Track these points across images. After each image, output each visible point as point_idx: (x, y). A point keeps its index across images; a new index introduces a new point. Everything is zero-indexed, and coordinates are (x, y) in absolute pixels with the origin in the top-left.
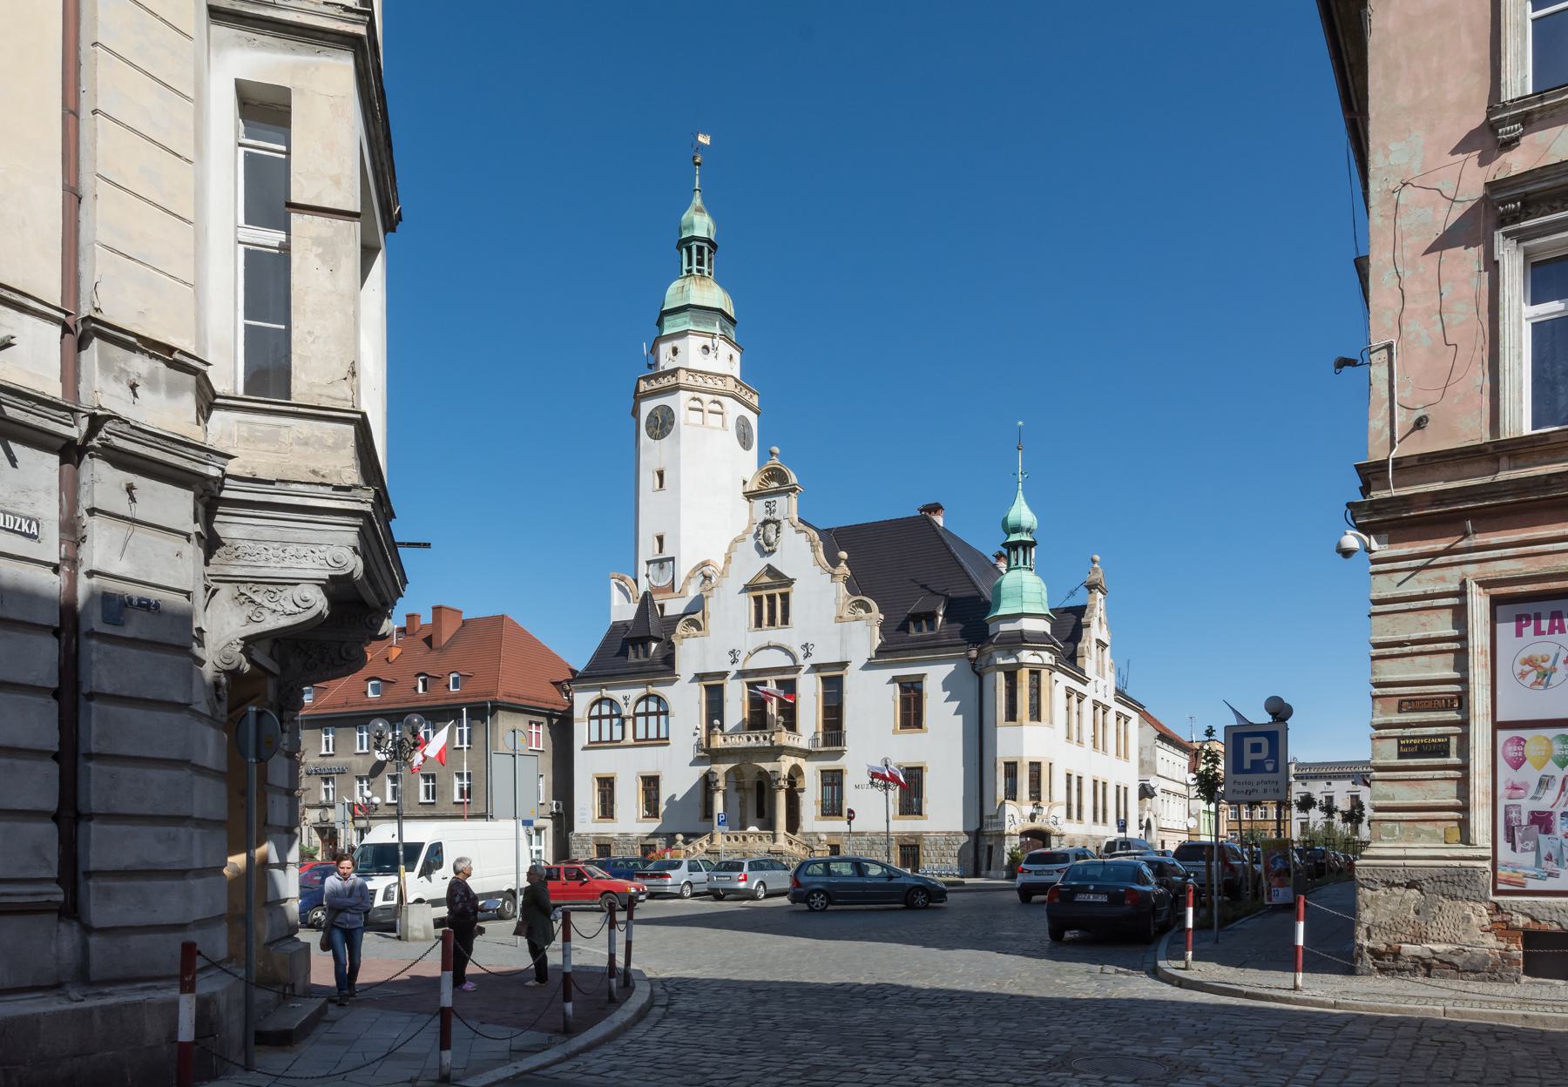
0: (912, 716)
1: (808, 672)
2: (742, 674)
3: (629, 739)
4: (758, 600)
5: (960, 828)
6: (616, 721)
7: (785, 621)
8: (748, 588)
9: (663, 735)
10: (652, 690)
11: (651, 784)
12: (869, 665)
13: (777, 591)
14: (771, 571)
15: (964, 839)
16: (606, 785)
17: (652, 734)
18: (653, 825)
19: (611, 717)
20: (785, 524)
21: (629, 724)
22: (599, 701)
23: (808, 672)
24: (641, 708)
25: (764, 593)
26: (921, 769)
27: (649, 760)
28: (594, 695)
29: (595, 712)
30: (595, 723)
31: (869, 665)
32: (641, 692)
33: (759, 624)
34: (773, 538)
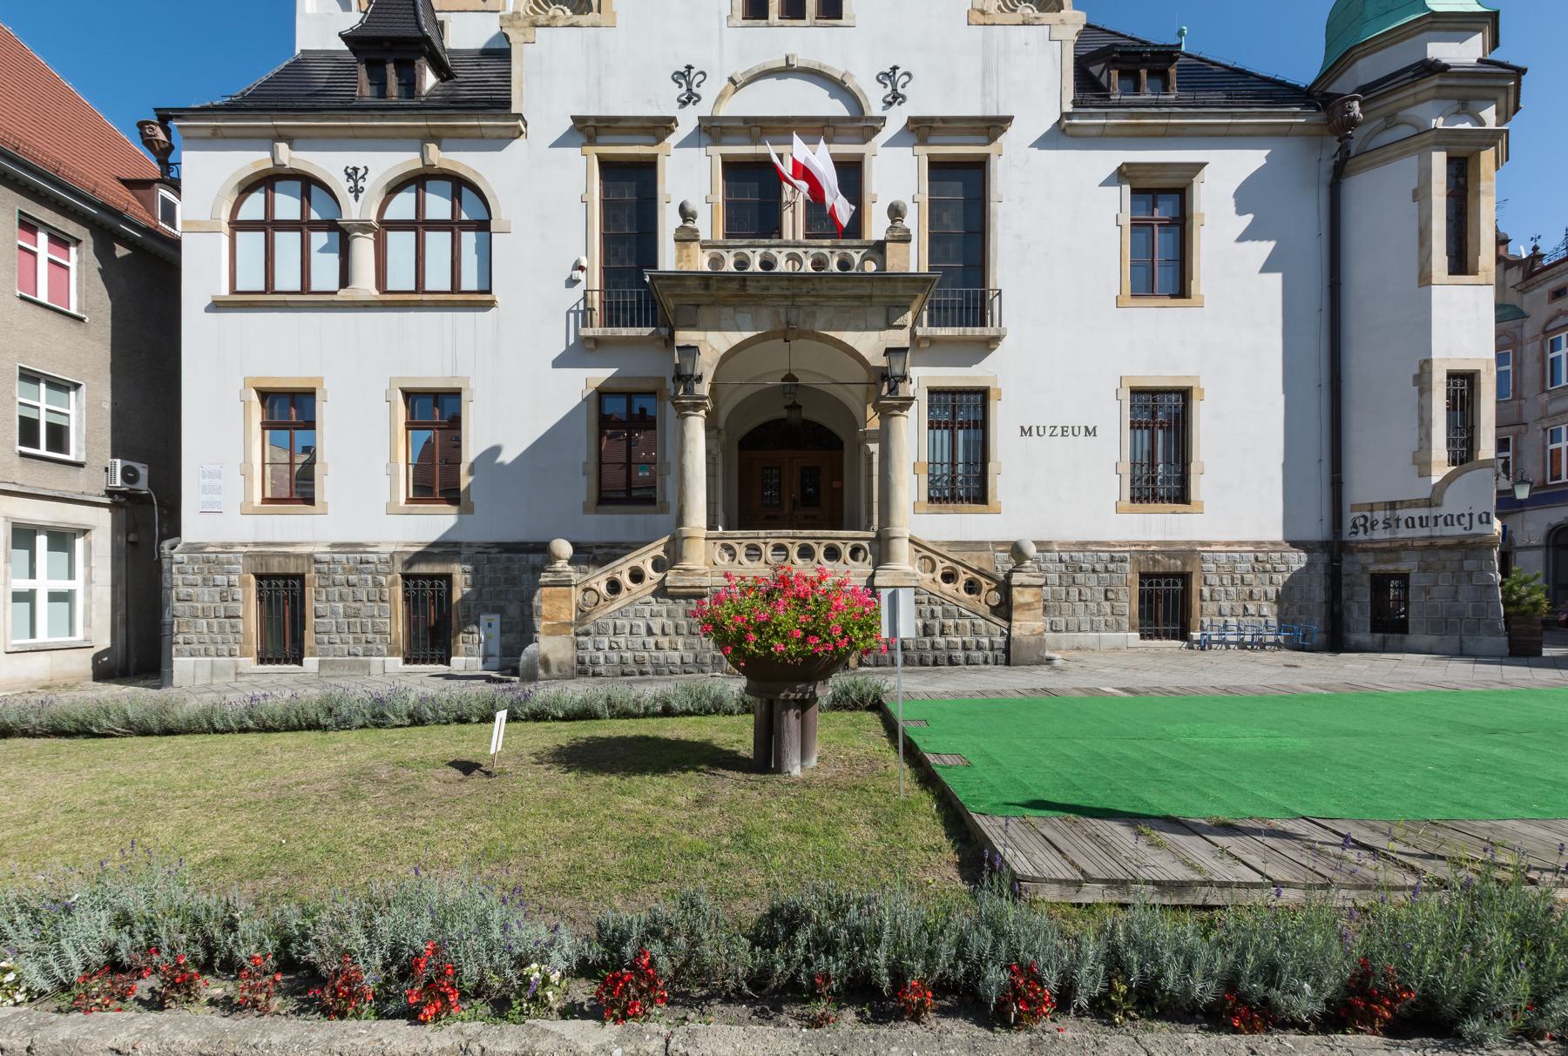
0: (1162, 259)
1: (893, 142)
2: (712, 130)
3: (364, 282)
5: (1277, 535)
6: (319, 239)
9: (470, 281)
10: (440, 157)
11: (434, 412)
12: (1061, 135)
15: (1298, 560)
16: (289, 409)
17: (437, 278)
18: (438, 522)
19: (303, 226)
21: (363, 248)
22: (266, 181)
23: (893, 142)
24: (403, 207)
26: (1185, 394)
27: (430, 348)
28: (253, 160)
29: (253, 208)
30: (252, 242)
31: (1061, 135)
32: (404, 160)
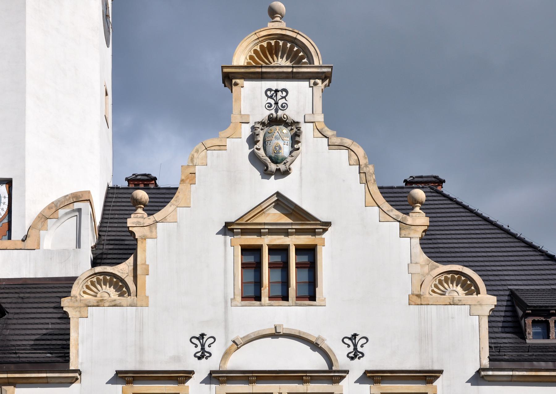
4: (251, 252)
7: (310, 294)
8: (228, 229)
13: (292, 241)
14: (281, 202)
20: (307, 130)
25: (266, 241)
33: (252, 293)
34: (285, 150)
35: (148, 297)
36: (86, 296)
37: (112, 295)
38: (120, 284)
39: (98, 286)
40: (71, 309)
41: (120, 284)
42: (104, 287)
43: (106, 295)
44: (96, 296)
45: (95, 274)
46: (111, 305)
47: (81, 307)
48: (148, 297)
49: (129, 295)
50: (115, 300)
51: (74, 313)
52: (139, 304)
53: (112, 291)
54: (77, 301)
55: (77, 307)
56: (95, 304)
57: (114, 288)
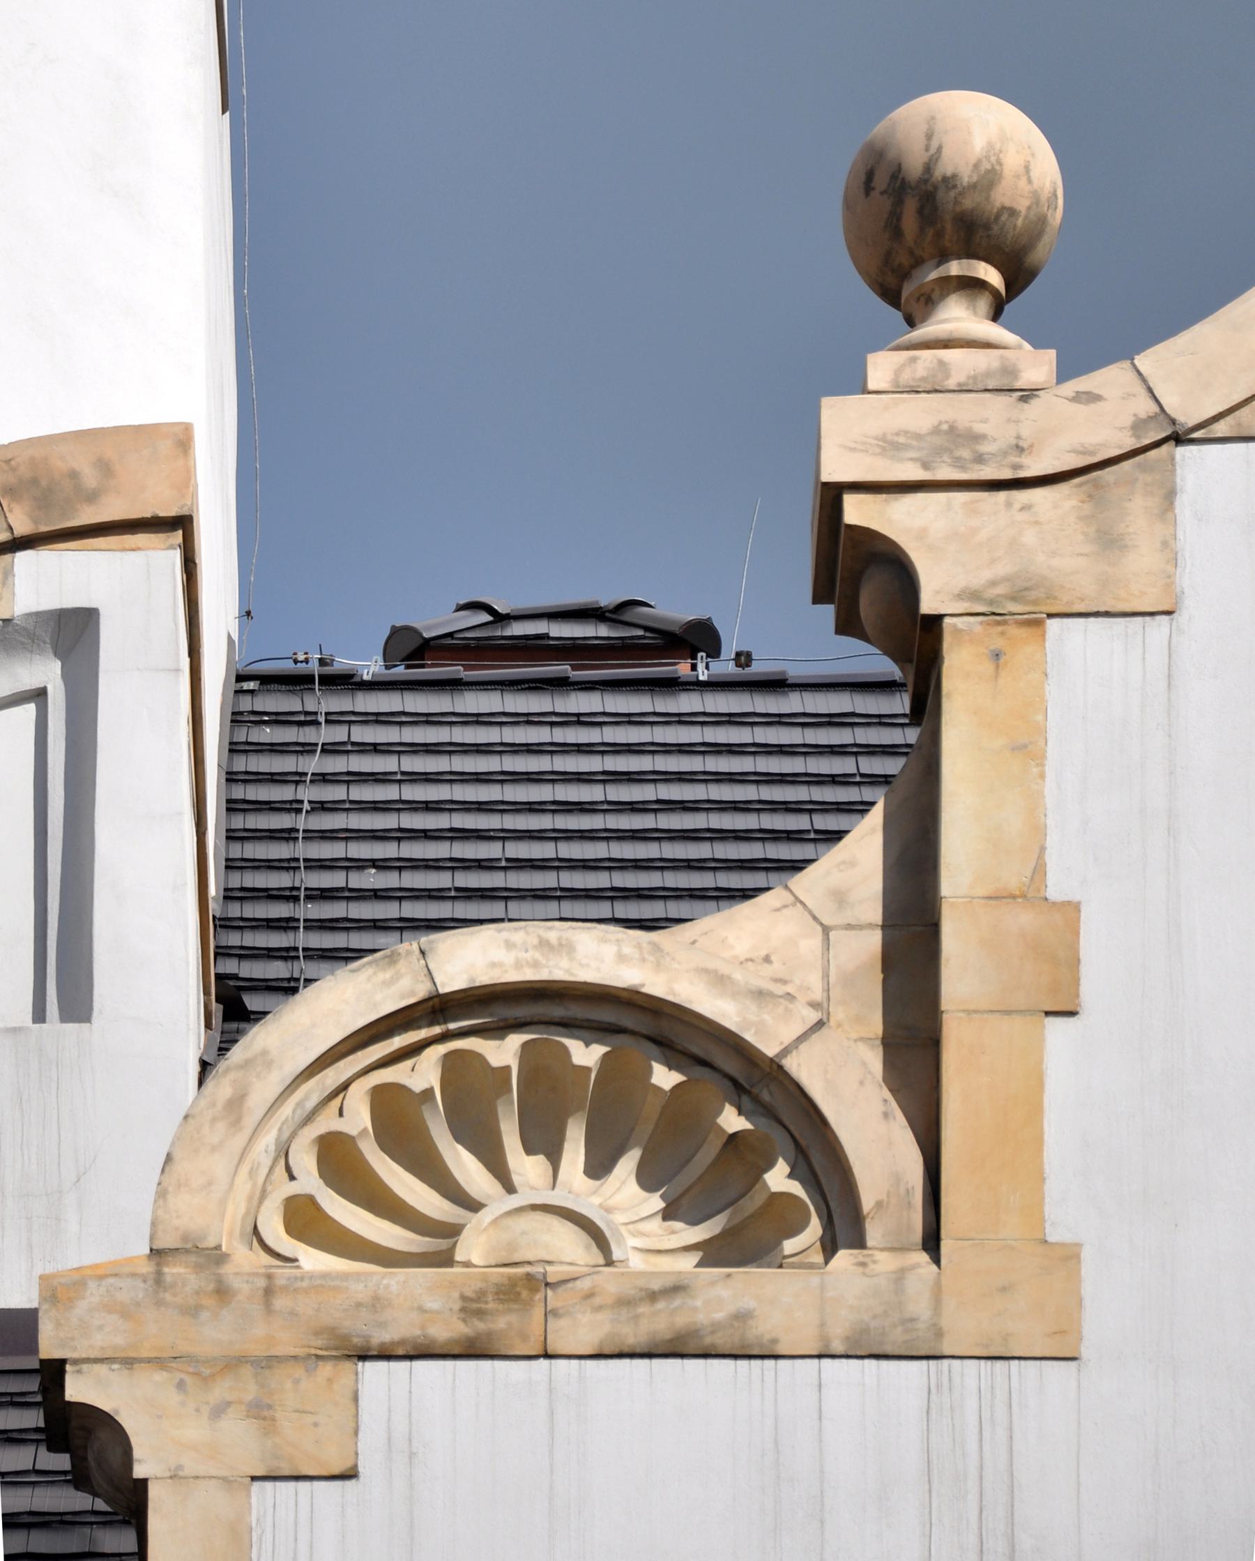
35: (1069, 1256)
36: (313, 1260)
37: (627, 1248)
38: (732, 1121)
39: (466, 1167)
40: (153, 1383)
41: (732, 1121)
42: (528, 1168)
43: (564, 1247)
44: (444, 1259)
45: (438, 1008)
46: (633, 1336)
47: (269, 1362)
48: (1069, 1256)
49: (844, 1227)
50: (676, 1289)
51: (194, 1430)
52: (962, 1329)
53: (624, 1200)
54: (222, 1292)
55: (232, 1364)
56: (445, 1330)
57: (647, 1179)
